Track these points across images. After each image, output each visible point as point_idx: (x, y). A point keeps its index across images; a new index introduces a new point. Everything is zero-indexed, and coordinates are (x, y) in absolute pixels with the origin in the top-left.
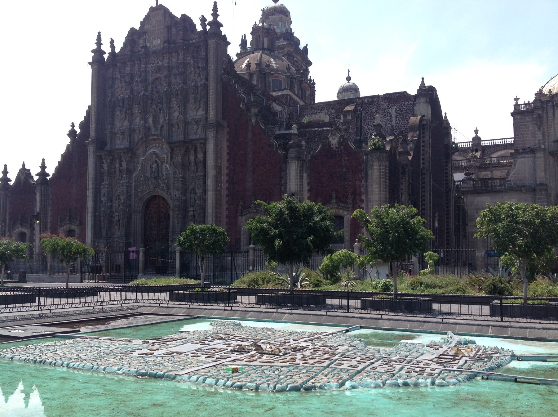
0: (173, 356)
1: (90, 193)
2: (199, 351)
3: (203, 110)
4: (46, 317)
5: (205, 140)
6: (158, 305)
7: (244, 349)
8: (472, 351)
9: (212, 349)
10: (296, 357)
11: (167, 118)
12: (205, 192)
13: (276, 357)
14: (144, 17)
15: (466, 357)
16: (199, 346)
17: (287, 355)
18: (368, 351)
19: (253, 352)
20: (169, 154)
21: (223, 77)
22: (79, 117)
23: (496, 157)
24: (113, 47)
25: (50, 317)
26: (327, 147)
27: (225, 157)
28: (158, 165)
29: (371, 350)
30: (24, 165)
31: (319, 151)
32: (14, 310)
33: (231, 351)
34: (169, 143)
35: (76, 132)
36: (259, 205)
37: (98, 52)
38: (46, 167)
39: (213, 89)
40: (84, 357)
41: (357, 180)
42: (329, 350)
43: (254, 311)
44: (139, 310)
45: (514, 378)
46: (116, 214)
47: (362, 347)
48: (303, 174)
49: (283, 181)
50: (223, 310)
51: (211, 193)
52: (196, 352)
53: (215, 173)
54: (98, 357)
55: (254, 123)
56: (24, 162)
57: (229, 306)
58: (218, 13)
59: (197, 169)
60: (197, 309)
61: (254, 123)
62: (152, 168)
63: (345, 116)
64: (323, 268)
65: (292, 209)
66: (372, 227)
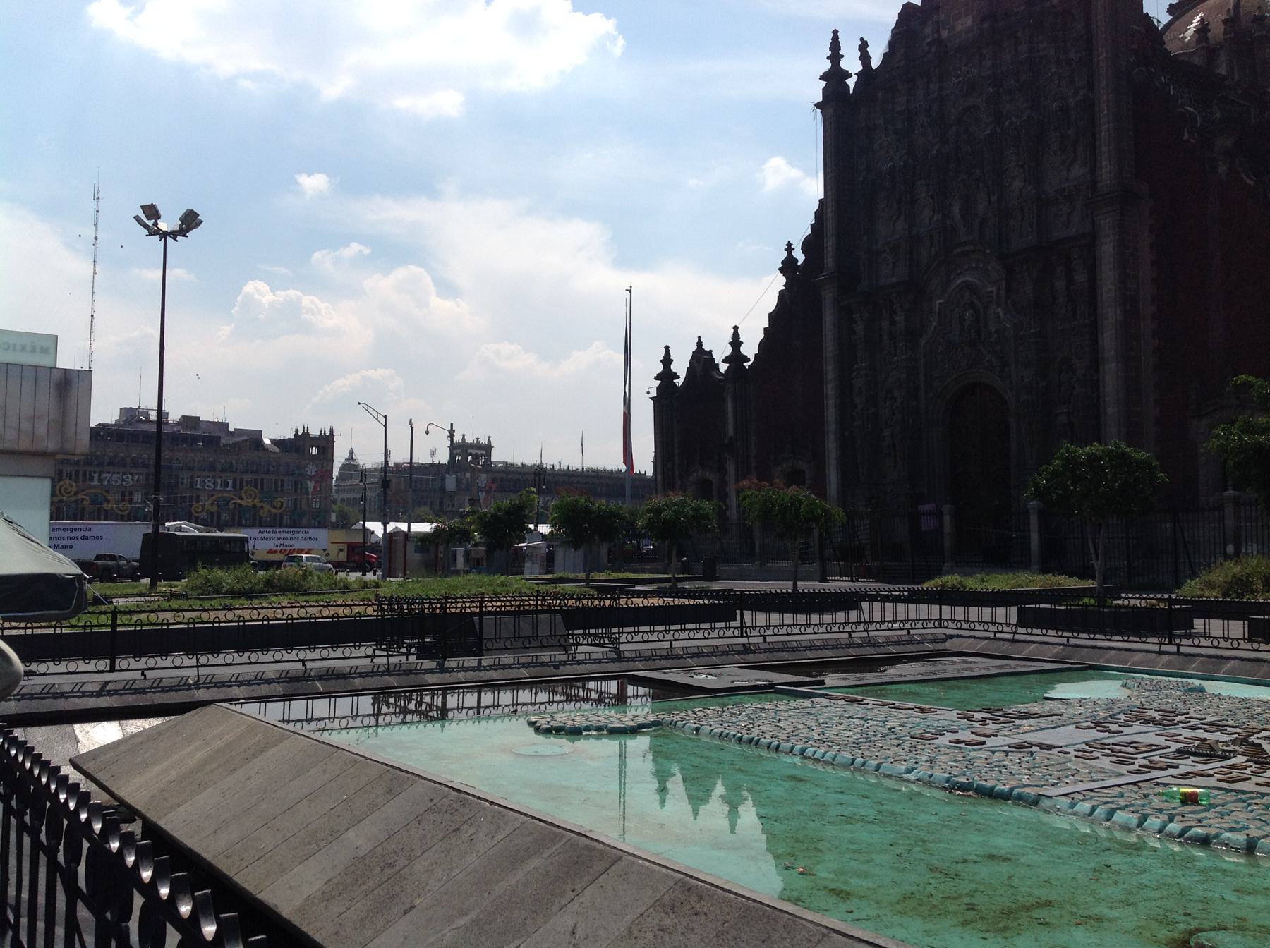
0: (1032, 753)
1: (830, 390)
2: (1095, 745)
4: (760, 651)
6: (992, 635)
7: (1212, 749)
9: (1128, 744)
11: (994, 198)
12: (1096, 364)
16: (1094, 734)
19: (1240, 760)
22: (800, 229)
24: (865, 57)
25: (765, 651)
30: (700, 343)
33: (1179, 751)
35: (797, 260)
37: (834, 77)
38: (742, 343)
40: (836, 737)
43: (1241, 659)
44: (949, 645)
50: (1155, 652)
51: (1114, 365)
52: (1087, 748)
54: (864, 740)
56: (699, 337)
57: (1170, 643)
58: (840, 52)
60: (1087, 647)
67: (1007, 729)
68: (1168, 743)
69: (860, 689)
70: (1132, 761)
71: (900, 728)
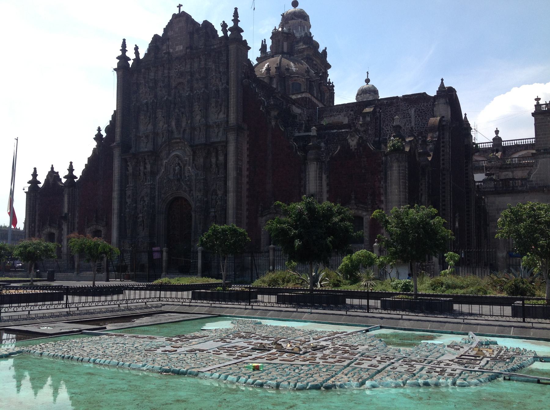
0: (196, 354)
2: (221, 348)
3: (224, 114)
4: (75, 314)
5: (227, 142)
6: (181, 303)
7: (264, 347)
8: (493, 351)
9: (233, 347)
10: (316, 356)
11: (189, 122)
12: (226, 192)
13: (296, 355)
14: (167, 24)
15: (488, 357)
16: (220, 344)
17: (308, 354)
18: (388, 351)
19: (274, 351)
21: (244, 81)
22: (105, 121)
24: (137, 53)
25: (78, 314)
27: (245, 159)
28: (180, 167)
29: (391, 350)
30: (52, 168)
32: (43, 308)
33: (252, 349)
34: (191, 146)
35: (103, 136)
36: (279, 205)
37: (123, 59)
39: (234, 93)
40: (110, 353)
41: (376, 181)
42: (349, 349)
43: (274, 311)
44: (163, 309)
45: (536, 380)
46: (141, 215)
47: (383, 347)
48: (322, 175)
50: (244, 309)
52: (218, 350)
53: (235, 175)
54: (124, 353)
56: (52, 165)
57: (249, 305)
59: (218, 172)
60: (218, 307)
61: (274, 127)
62: (174, 170)
63: (364, 118)
64: (342, 268)
67: (186, 344)
69: (122, 330)
70: (235, 354)
71: (140, 347)
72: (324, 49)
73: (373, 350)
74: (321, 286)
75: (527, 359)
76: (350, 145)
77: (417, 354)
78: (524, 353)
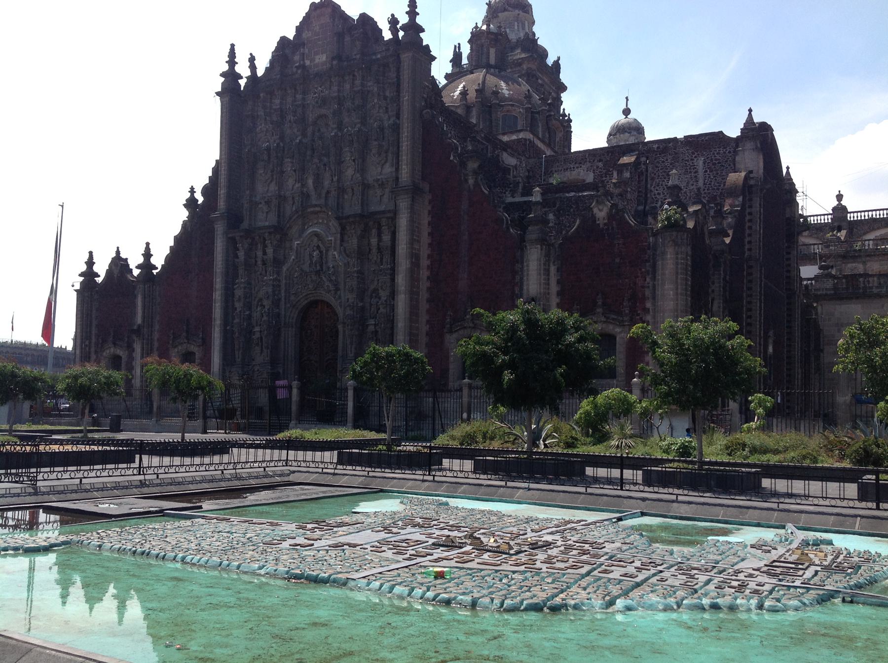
0: (344, 550)
1: (218, 295)
2: (384, 543)
3: (392, 166)
4: (152, 484)
6: (320, 470)
7: (453, 542)
8: (826, 556)
11: (335, 179)
12: (393, 294)
13: (504, 556)
14: (301, 19)
15: (816, 565)
16: (383, 535)
17: (522, 555)
18: (653, 553)
19: (468, 548)
20: (339, 235)
21: (424, 112)
22: (201, 178)
23: (873, 240)
24: (253, 67)
25: (157, 485)
26: (590, 222)
27: (425, 239)
28: (321, 252)
29: (659, 550)
30: (118, 252)
31: (576, 229)
33: (433, 544)
34: (338, 218)
35: (198, 201)
36: (479, 315)
37: (231, 76)
38: (152, 255)
39: (408, 133)
40: (209, 547)
41: (638, 277)
42: (590, 548)
43: (470, 484)
44: (292, 478)
46: (257, 329)
47: (644, 546)
48: (549, 266)
49: (518, 278)
50: (420, 480)
51: (403, 296)
52: (378, 544)
55: (472, 187)
56: (118, 248)
57: (429, 475)
59: (382, 259)
60: (380, 478)
61: (472, 187)
62: (311, 256)
64: (580, 418)
65: (531, 323)
66: (662, 352)
68: (427, 539)
69: (228, 511)
70: (406, 552)
71: (256, 538)
72: (556, 59)
73: (628, 549)
74: (546, 446)
75: (881, 569)
76: (595, 217)
77: (700, 559)
78: (877, 560)
